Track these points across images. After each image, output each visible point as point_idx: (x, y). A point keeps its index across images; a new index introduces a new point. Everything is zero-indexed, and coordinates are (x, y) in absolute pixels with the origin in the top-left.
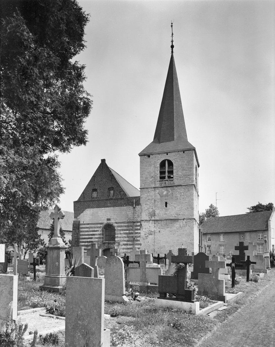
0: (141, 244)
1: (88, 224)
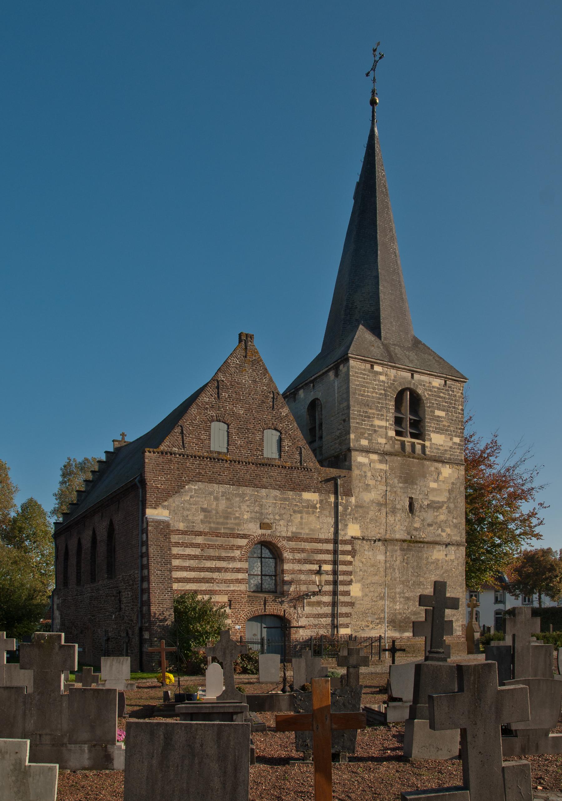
0: (352, 604)
1: (200, 534)
